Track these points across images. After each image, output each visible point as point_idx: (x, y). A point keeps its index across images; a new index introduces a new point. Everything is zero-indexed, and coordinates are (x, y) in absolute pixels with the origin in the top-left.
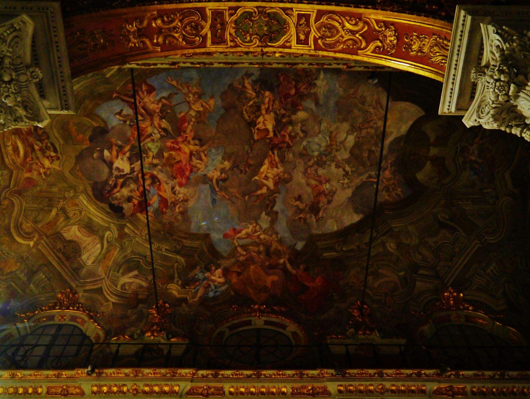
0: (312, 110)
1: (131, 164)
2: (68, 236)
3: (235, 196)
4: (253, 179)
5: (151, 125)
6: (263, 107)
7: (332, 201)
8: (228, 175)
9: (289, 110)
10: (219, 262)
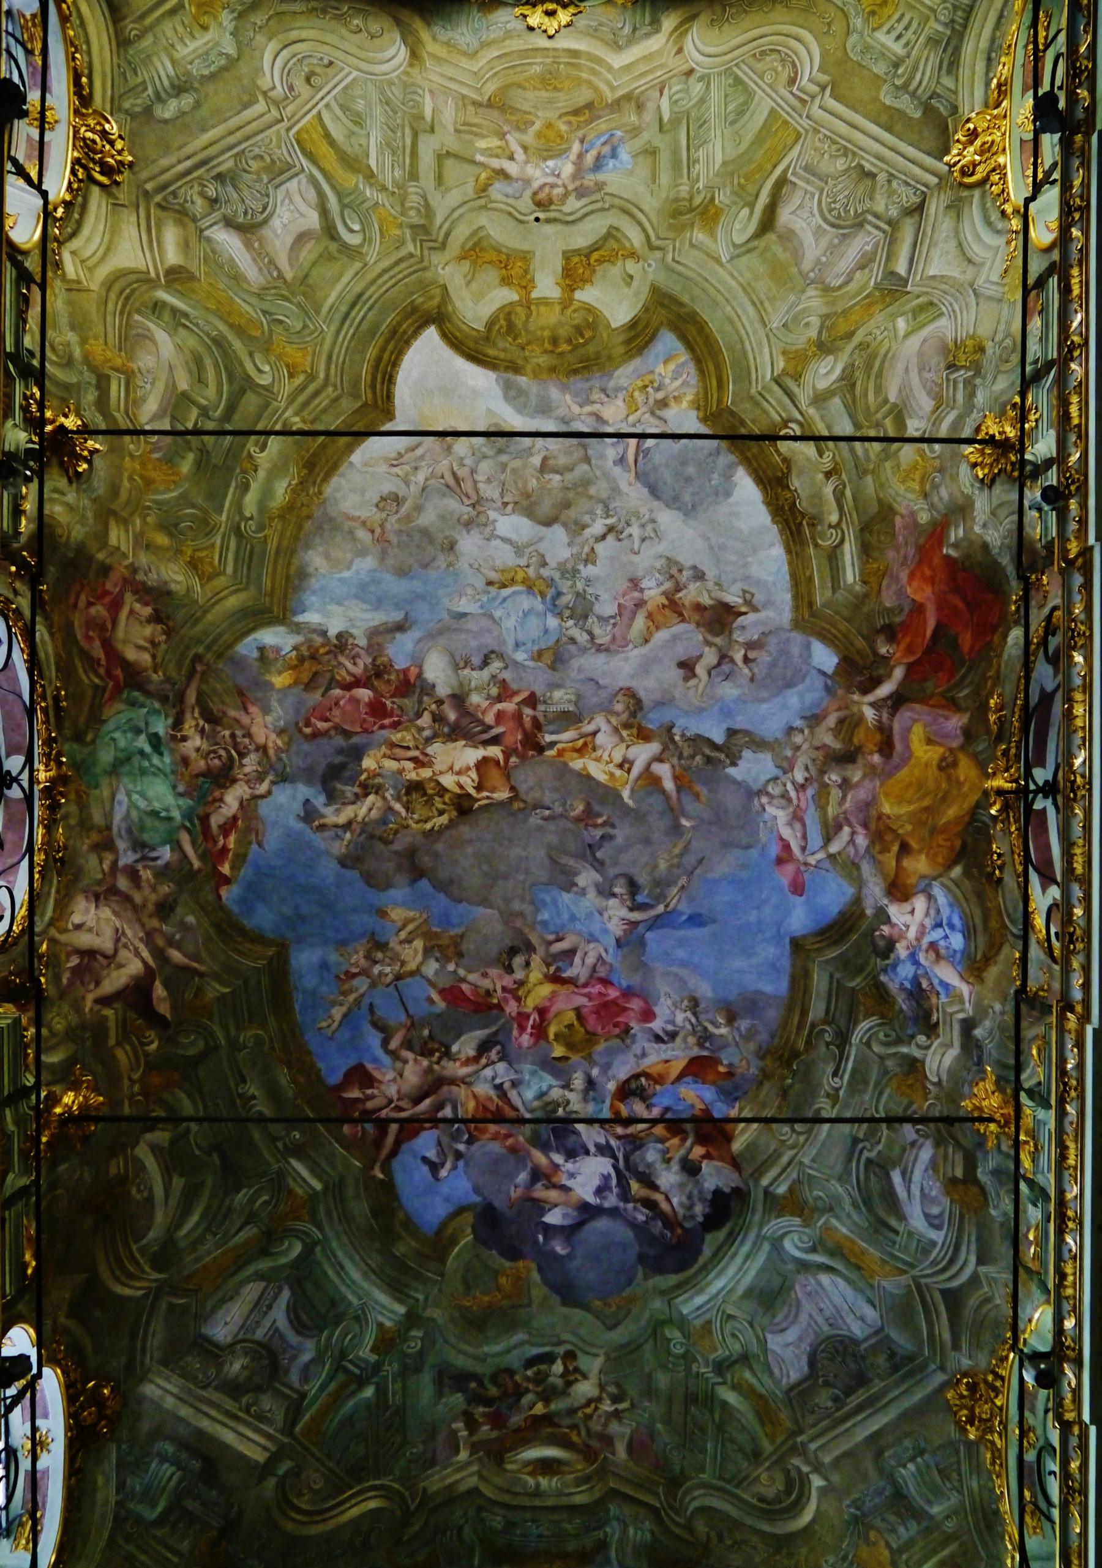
0: (420, 640)
1: (587, 1153)
2: (795, 1371)
3: (681, 855)
4: (630, 803)
5: (469, 1084)
6: (413, 776)
7: (695, 568)
8: (617, 876)
9: (420, 702)
10: (869, 912)
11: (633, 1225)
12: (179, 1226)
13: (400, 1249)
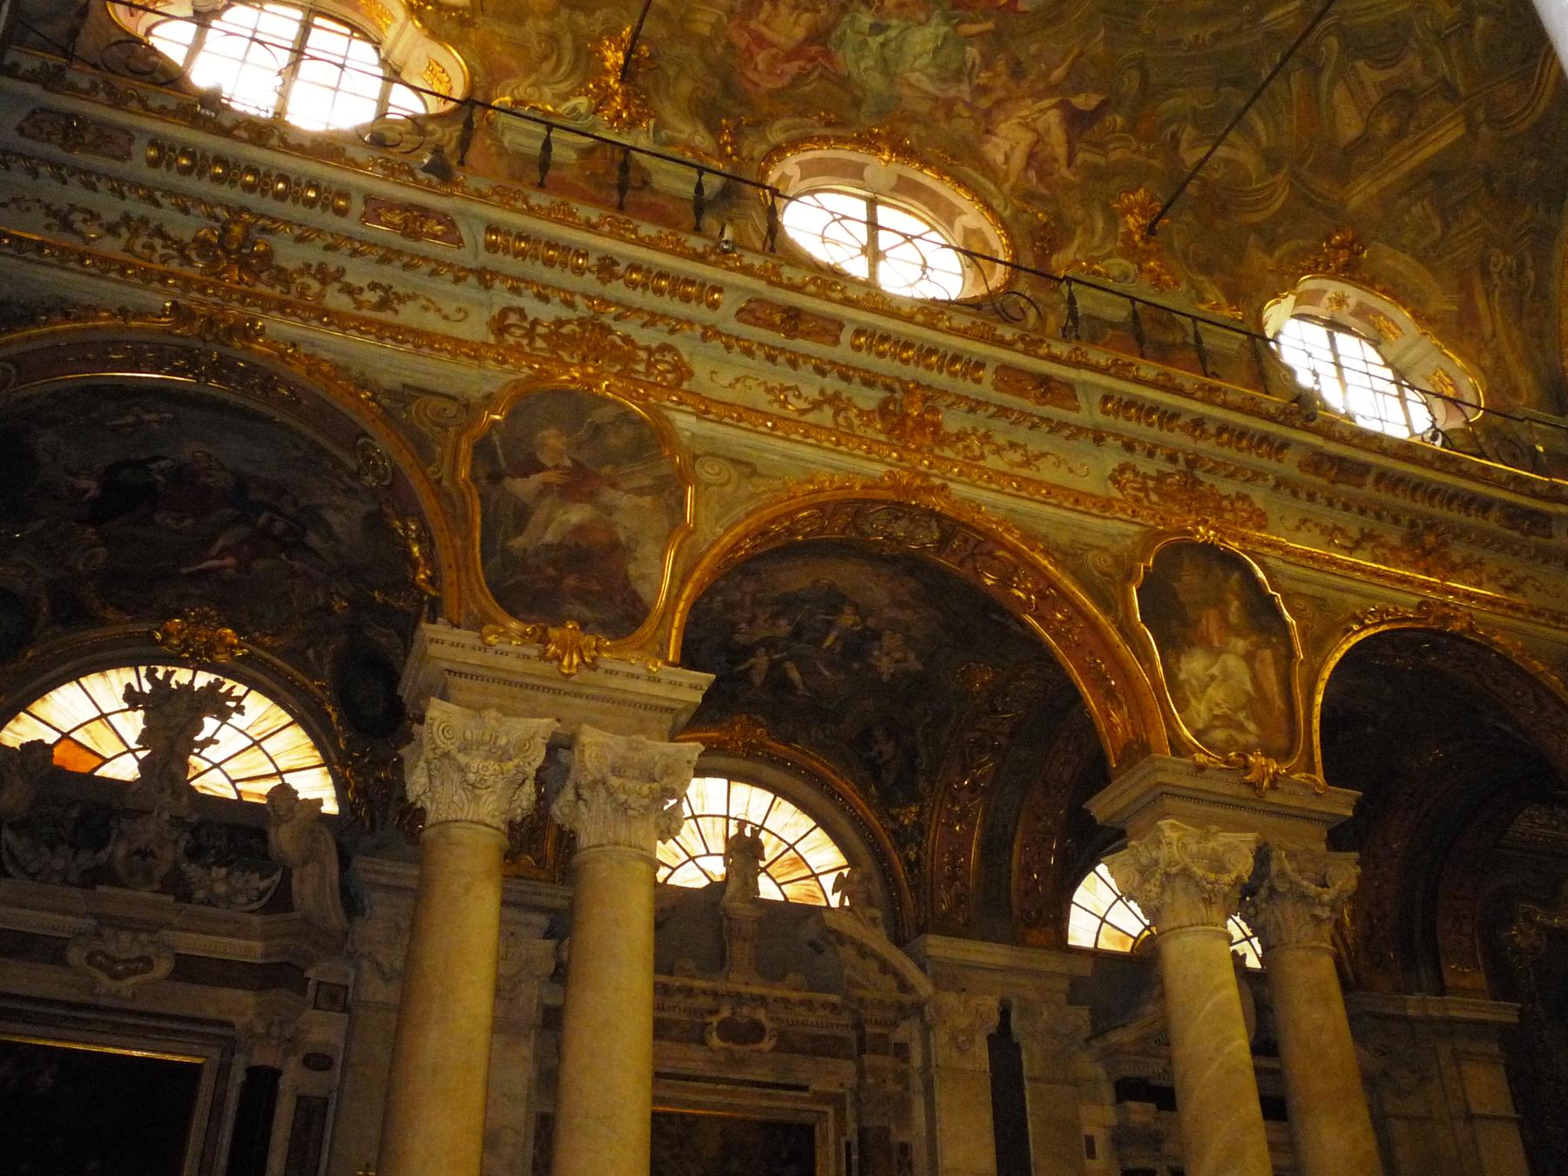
12: (1258, 142)
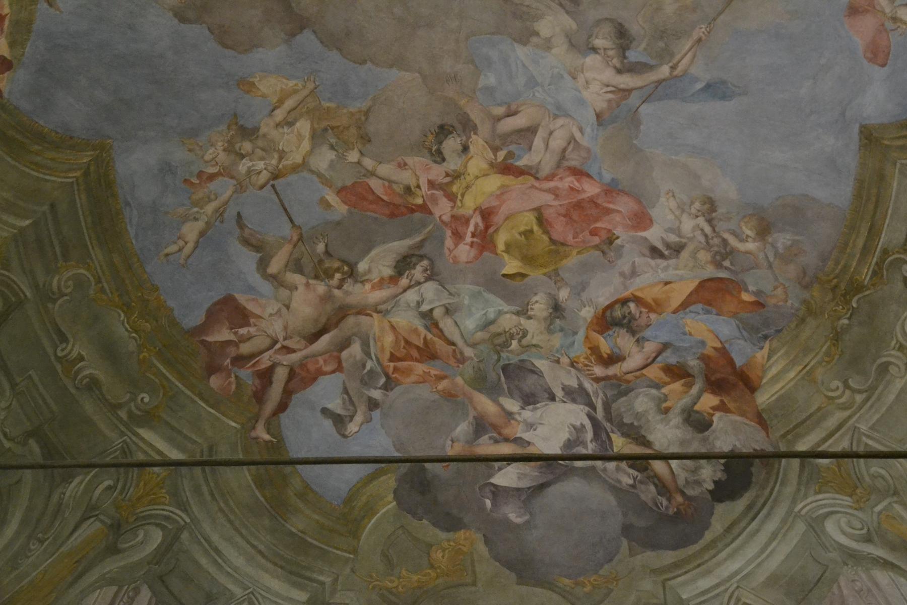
1: (552, 398)
8: (598, 22)
11: (616, 489)
13: (296, 524)
